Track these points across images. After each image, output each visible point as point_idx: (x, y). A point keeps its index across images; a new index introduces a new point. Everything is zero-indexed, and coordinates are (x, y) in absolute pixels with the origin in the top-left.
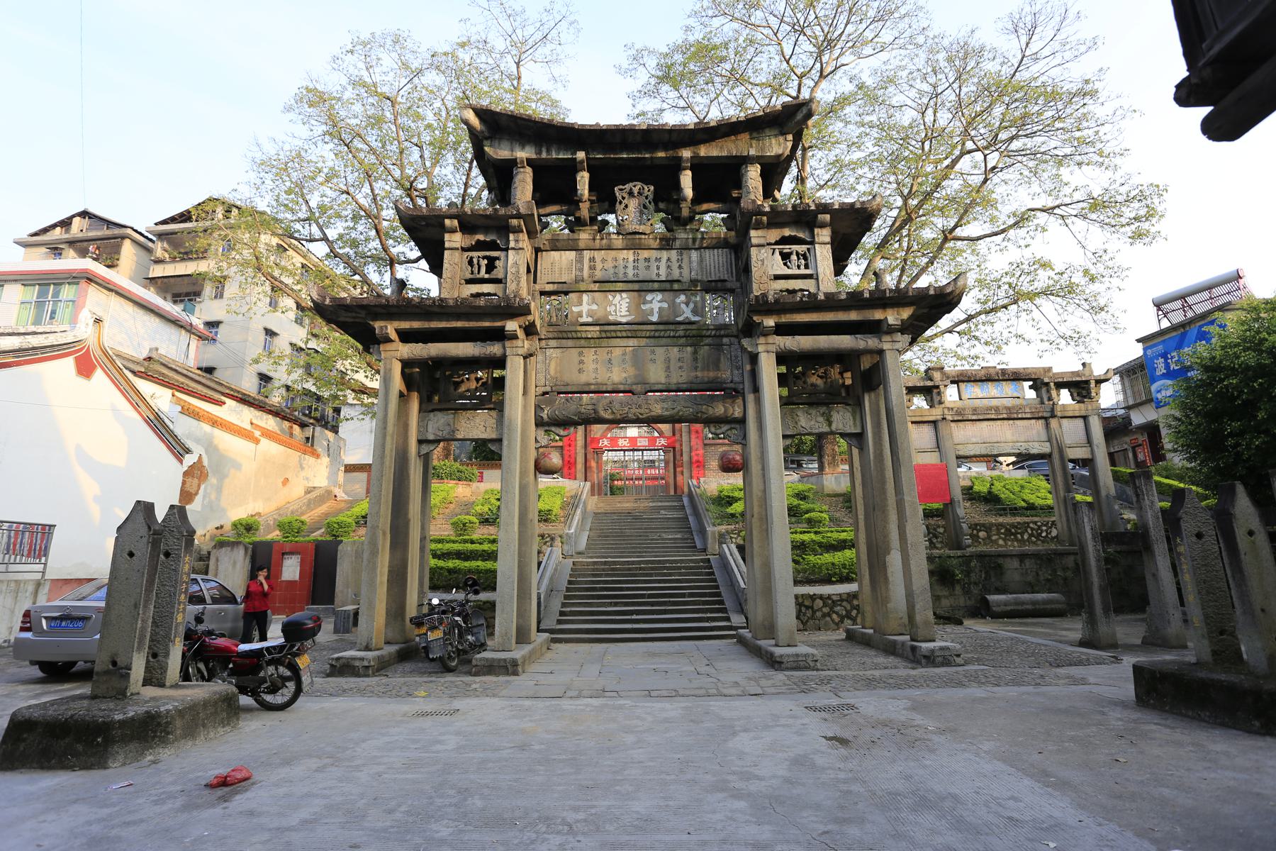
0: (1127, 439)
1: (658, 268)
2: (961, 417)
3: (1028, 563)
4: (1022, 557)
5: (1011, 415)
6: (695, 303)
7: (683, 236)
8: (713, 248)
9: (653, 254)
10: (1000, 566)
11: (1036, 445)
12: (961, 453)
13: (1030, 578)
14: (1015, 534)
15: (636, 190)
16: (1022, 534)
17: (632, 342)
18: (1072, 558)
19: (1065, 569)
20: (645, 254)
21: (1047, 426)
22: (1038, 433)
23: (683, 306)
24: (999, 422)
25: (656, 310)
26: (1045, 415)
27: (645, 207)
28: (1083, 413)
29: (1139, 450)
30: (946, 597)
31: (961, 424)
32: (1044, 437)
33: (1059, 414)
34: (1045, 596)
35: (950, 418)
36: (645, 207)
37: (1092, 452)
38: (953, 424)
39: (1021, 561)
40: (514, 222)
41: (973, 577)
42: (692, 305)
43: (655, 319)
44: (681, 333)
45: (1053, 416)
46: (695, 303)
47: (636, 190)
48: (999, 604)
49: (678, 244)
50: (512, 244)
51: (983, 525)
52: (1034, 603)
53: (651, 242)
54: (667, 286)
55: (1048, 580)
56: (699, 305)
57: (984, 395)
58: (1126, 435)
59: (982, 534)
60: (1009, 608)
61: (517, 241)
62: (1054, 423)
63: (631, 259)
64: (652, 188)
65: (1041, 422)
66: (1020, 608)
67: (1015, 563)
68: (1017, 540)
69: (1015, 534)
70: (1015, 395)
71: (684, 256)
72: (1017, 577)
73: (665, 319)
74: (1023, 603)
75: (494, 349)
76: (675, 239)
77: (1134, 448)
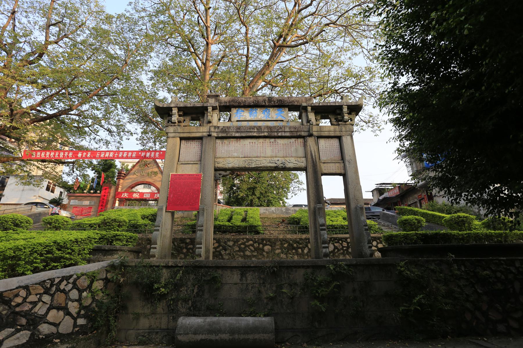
0: (416, 196)
2: (226, 136)
3: (250, 277)
4: (244, 270)
5: (272, 134)
10: (214, 280)
11: (293, 160)
12: (220, 165)
13: (250, 296)
14: (296, 249)
16: (302, 249)
18: (302, 272)
19: (292, 285)
21: (305, 145)
22: (296, 150)
24: (261, 140)
26: (303, 134)
28: (338, 134)
29: (423, 202)
30: (146, 316)
31: (226, 141)
32: (301, 152)
33: (315, 134)
34: (250, 320)
35: (215, 135)
37: (345, 166)
38: (218, 141)
39: (243, 275)
41: (184, 292)
45: (311, 135)
48: (187, 331)
51: (269, 240)
52: (233, 330)
55: (271, 299)
57: (252, 118)
58: (416, 193)
59: (267, 248)
60: (199, 337)
62: (311, 141)
65: (300, 140)
66: (213, 337)
67: (236, 277)
68: (297, 254)
69: (296, 249)
70: (280, 118)
72: (235, 293)
74: (219, 331)
77: (420, 201)
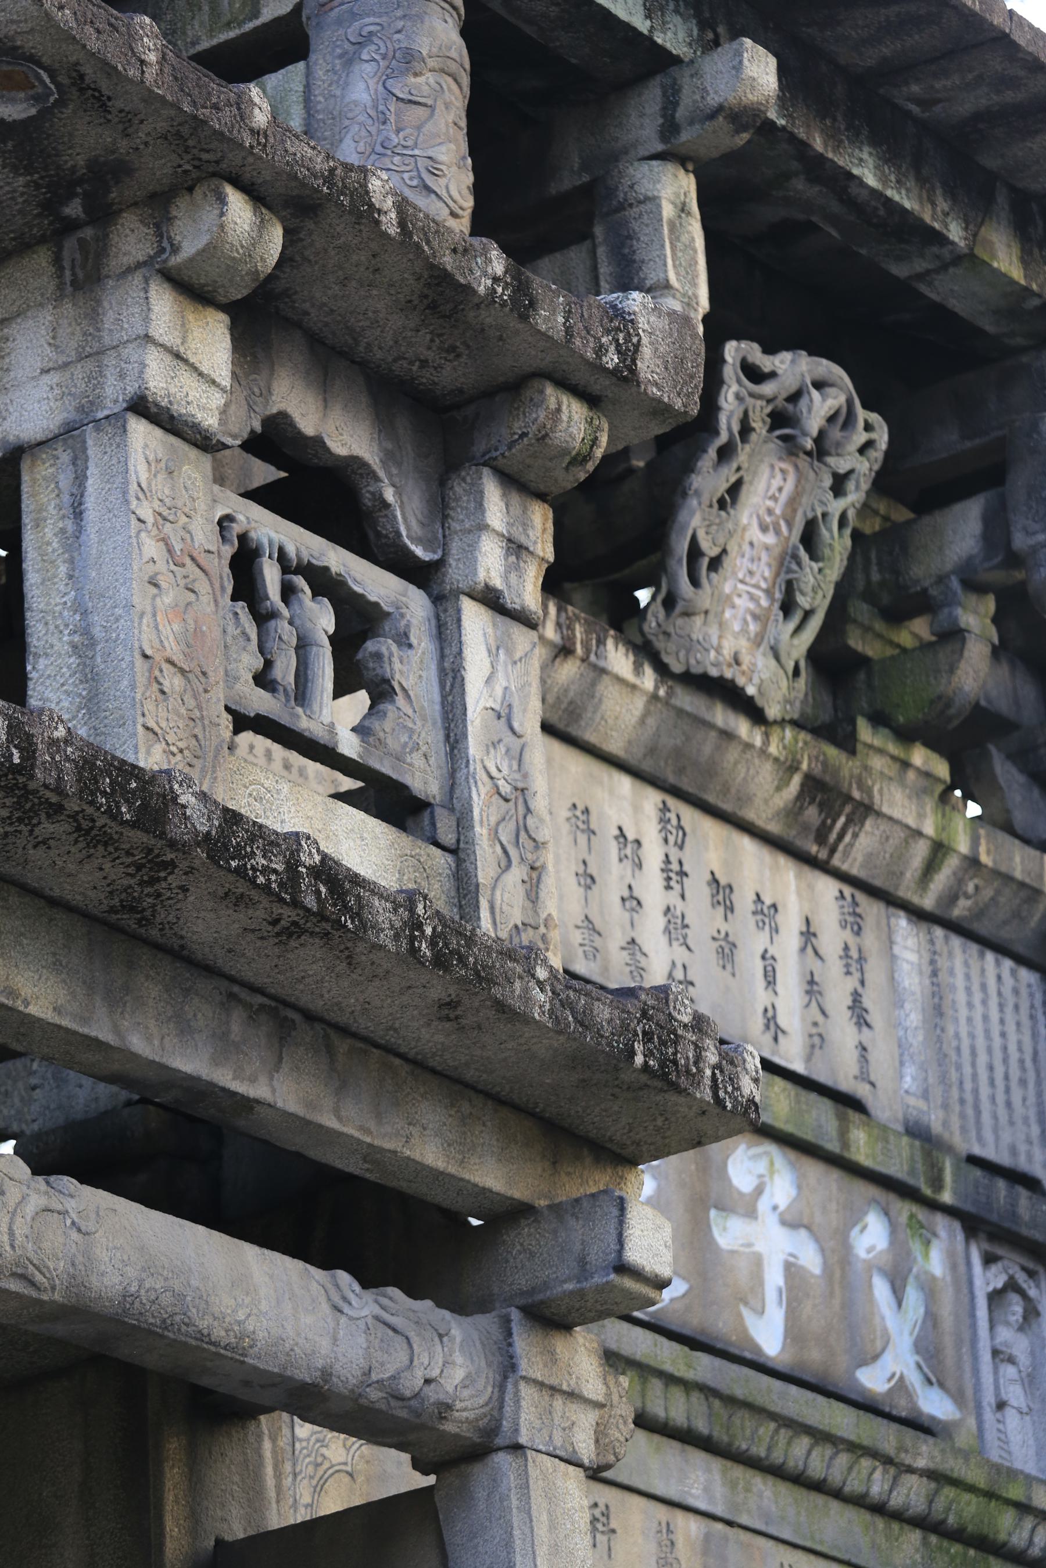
1: (770, 979)
6: (930, 1290)
7: (898, 803)
8: (986, 943)
9: (755, 868)
15: (817, 410)
17: (699, 1479)
20: (712, 845)
23: (881, 1289)
25: (774, 1278)
27: (809, 538)
36: (809, 538)
40: (572, 422)
42: (913, 1296)
43: (769, 1336)
44: (911, 1494)
46: (930, 1290)
47: (817, 410)
49: (862, 849)
50: (490, 563)
53: (765, 776)
54: (819, 1120)
56: (946, 1310)
61: (516, 548)
63: (653, 853)
64: (882, 437)
71: (870, 940)
73: (815, 1355)
75: (444, 1359)
76: (866, 810)
